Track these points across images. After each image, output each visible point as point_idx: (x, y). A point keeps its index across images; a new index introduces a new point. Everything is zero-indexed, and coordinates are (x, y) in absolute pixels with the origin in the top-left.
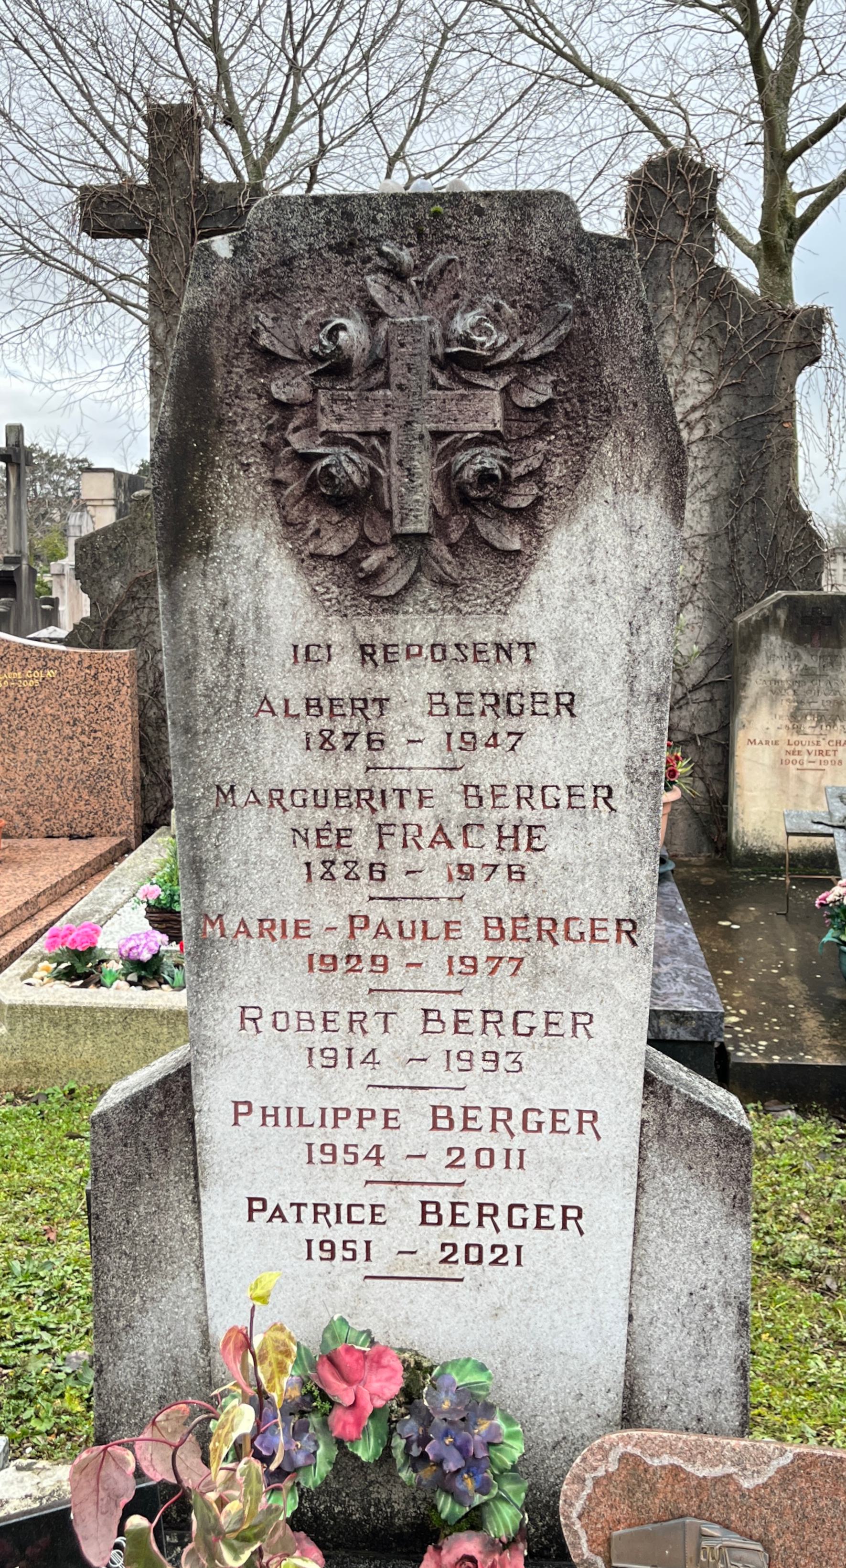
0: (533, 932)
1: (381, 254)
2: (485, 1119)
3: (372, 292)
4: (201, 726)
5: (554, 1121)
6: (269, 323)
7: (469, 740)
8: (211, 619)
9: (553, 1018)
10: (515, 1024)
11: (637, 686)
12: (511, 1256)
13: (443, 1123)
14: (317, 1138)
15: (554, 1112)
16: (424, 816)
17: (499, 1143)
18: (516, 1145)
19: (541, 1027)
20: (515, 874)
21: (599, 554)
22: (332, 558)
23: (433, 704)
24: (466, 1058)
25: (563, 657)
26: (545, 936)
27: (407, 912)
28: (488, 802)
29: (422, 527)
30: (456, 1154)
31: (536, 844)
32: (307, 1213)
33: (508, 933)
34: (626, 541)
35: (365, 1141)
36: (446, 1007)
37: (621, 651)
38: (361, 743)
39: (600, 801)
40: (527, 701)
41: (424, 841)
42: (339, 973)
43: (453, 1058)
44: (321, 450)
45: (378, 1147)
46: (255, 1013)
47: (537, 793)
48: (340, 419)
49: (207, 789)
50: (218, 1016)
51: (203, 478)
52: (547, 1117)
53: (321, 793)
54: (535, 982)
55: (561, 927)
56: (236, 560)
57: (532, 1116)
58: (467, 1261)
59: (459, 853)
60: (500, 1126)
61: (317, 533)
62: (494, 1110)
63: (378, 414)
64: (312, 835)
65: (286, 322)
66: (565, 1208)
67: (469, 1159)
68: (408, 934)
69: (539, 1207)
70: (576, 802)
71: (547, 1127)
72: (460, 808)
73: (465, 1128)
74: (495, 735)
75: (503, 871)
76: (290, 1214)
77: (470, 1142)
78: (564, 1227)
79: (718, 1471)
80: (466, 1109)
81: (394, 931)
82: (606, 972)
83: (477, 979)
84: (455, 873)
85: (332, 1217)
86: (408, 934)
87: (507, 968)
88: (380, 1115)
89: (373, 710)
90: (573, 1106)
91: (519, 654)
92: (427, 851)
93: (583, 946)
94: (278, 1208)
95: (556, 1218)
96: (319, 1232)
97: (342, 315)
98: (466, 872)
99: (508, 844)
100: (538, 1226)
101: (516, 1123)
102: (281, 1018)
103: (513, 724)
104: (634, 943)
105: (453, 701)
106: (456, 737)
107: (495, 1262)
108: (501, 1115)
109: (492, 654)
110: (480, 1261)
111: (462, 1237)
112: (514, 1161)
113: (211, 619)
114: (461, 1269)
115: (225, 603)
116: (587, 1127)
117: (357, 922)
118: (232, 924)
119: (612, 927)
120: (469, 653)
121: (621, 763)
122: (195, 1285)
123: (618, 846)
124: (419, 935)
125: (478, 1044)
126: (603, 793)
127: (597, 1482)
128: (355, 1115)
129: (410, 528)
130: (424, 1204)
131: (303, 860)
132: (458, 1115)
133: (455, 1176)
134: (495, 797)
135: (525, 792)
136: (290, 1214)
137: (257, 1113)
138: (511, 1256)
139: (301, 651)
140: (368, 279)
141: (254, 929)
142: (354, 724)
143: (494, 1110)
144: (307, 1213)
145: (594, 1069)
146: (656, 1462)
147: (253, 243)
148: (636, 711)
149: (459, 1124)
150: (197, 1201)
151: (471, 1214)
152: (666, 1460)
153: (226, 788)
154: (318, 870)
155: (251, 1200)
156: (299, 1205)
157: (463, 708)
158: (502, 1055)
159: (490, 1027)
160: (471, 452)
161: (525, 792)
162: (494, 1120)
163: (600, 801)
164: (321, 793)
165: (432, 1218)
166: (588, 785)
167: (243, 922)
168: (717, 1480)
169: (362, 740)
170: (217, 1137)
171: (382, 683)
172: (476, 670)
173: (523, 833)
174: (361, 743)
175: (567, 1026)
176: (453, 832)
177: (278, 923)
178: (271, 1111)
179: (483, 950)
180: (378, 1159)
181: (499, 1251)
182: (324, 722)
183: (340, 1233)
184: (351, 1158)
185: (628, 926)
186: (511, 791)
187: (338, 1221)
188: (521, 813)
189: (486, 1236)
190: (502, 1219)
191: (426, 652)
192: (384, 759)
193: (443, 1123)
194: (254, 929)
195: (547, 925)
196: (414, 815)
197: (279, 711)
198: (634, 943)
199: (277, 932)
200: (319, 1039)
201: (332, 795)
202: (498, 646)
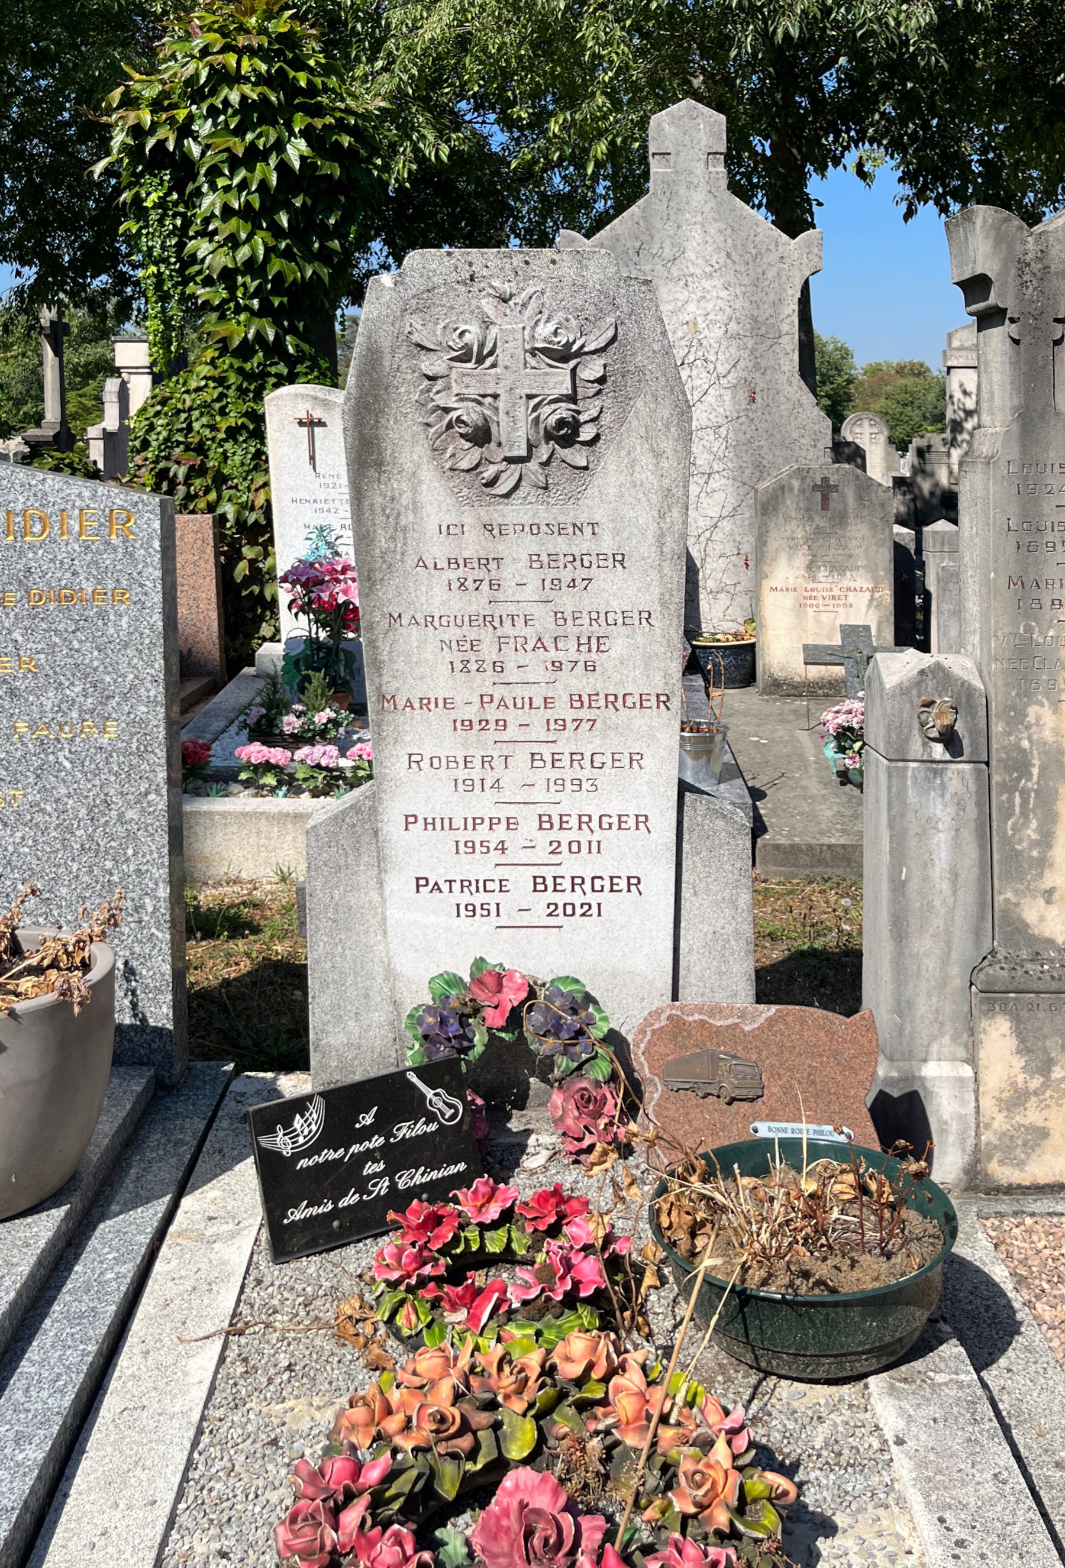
0: (602, 703)
1: (492, 287)
2: (574, 822)
3: (486, 310)
4: (379, 576)
5: (620, 822)
6: (419, 327)
7: (557, 584)
8: (383, 510)
9: (616, 757)
10: (592, 762)
11: (665, 549)
12: (594, 910)
13: (547, 825)
14: (462, 836)
15: (620, 816)
16: (528, 632)
17: (584, 836)
18: (595, 838)
19: (609, 763)
20: (590, 667)
21: (637, 468)
22: (463, 471)
23: (531, 561)
24: (560, 783)
25: (616, 532)
26: (610, 705)
27: (520, 691)
28: (570, 622)
29: (523, 452)
30: (555, 845)
31: (602, 648)
32: (456, 886)
33: (586, 704)
34: (654, 461)
35: (494, 839)
36: (546, 751)
37: (653, 528)
38: (485, 586)
39: (644, 621)
40: (594, 558)
41: (529, 646)
42: (474, 731)
43: (552, 784)
44: (455, 405)
45: (503, 842)
46: (418, 758)
47: (602, 616)
48: (467, 387)
49: (383, 615)
50: (393, 760)
51: (377, 421)
52: (615, 820)
53: (459, 618)
54: (605, 736)
55: (620, 699)
56: (400, 473)
57: (605, 820)
58: (565, 914)
59: (552, 654)
60: (584, 826)
61: (453, 455)
62: (580, 816)
63: (492, 384)
64: (454, 644)
65: (430, 326)
66: (629, 878)
67: (564, 847)
68: (519, 705)
69: (612, 878)
70: (627, 621)
71: (615, 826)
72: (553, 626)
73: (561, 828)
74: (573, 580)
75: (581, 665)
76: (445, 887)
77: (565, 837)
78: (629, 890)
79: (730, 1021)
80: (561, 816)
81: (510, 704)
82: (651, 727)
83: (566, 733)
84: (550, 667)
85: (473, 888)
86: (519, 705)
87: (585, 726)
88: (504, 822)
89: (493, 565)
90: (632, 811)
91: (588, 530)
92: (530, 654)
93: (636, 711)
94: (436, 884)
95: (623, 884)
96: (465, 898)
97: (466, 323)
98: (556, 665)
99: (583, 648)
100: (612, 890)
101: (594, 824)
102: (436, 761)
103: (585, 573)
104: (668, 708)
105: (544, 558)
106: (547, 583)
107: (583, 915)
108: (585, 819)
109: (570, 530)
110: (573, 914)
111: (560, 899)
112: (594, 849)
113: (383, 510)
114: (561, 920)
115: (393, 499)
116: (641, 825)
117: (486, 699)
118: (401, 704)
119: (654, 699)
120: (555, 529)
121: (656, 598)
122: (379, 938)
123: (655, 648)
124: (527, 706)
125: (568, 774)
126: (645, 615)
127: (654, 1032)
128: (487, 822)
129: (516, 453)
130: (535, 878)
131: (448, 660)
132: (556, 820)
133: (555, 859)
134: (574, 619)
135: (594, 616)
136: (445, 887)
137: (421, 822)
138: (594, 910)
139: (444, 529)
140: (484, 301)
141: (417, 705)
142: (481, 574)
143: (580, 816)
144: (456, 886)
145: (645, 788)
146: (691, 1019)
147: (407, 279)
148: (666, 564)
149: (557, 826)
150: (381, 884)
151: (567, 884)
152: (697, 1017)
153: (396, 615)
154: (458, 666)
155: (418, 879)
156: (450, 882)
157: (553, 564)
158: (584, 780)
159: (575, 764)
160: (553, 406)
161: (594, 616)
162: (580, 823)
163: (644, 621)
164: (459, 618)
165: (541, 887)
166: (636, 611)
167: (408, 700)
168: (728, 1027)
169: (486, 583)
170: (394, 838)
171: (501, 548)
172: (560, 539)
173: (594, 641)
174: (485, 586)
175: (626, 761)
176: (548, 642)
177: (433, 701)
178: (430, 821)
179: (570, 715)
180: (503, 850)
181: (586, 907)
182: (460, 572)
183: (479, 899)
184: (485, 850)
185: (663, 698)
186: (585, 615)
187: (477, 891)
188: (592, 629)
189: (577, 898)
190: (587, 886)
191: (527, 529)
192: (500, 596)
193: (547, 825)
194: (417, 705)
195: (611, 698)
196: (520, 629)
197: (431, 566)
198: (668, 708)
199: (432, 706)
200: (461, 774)
201: (466, 619)
202: (575, 525)
